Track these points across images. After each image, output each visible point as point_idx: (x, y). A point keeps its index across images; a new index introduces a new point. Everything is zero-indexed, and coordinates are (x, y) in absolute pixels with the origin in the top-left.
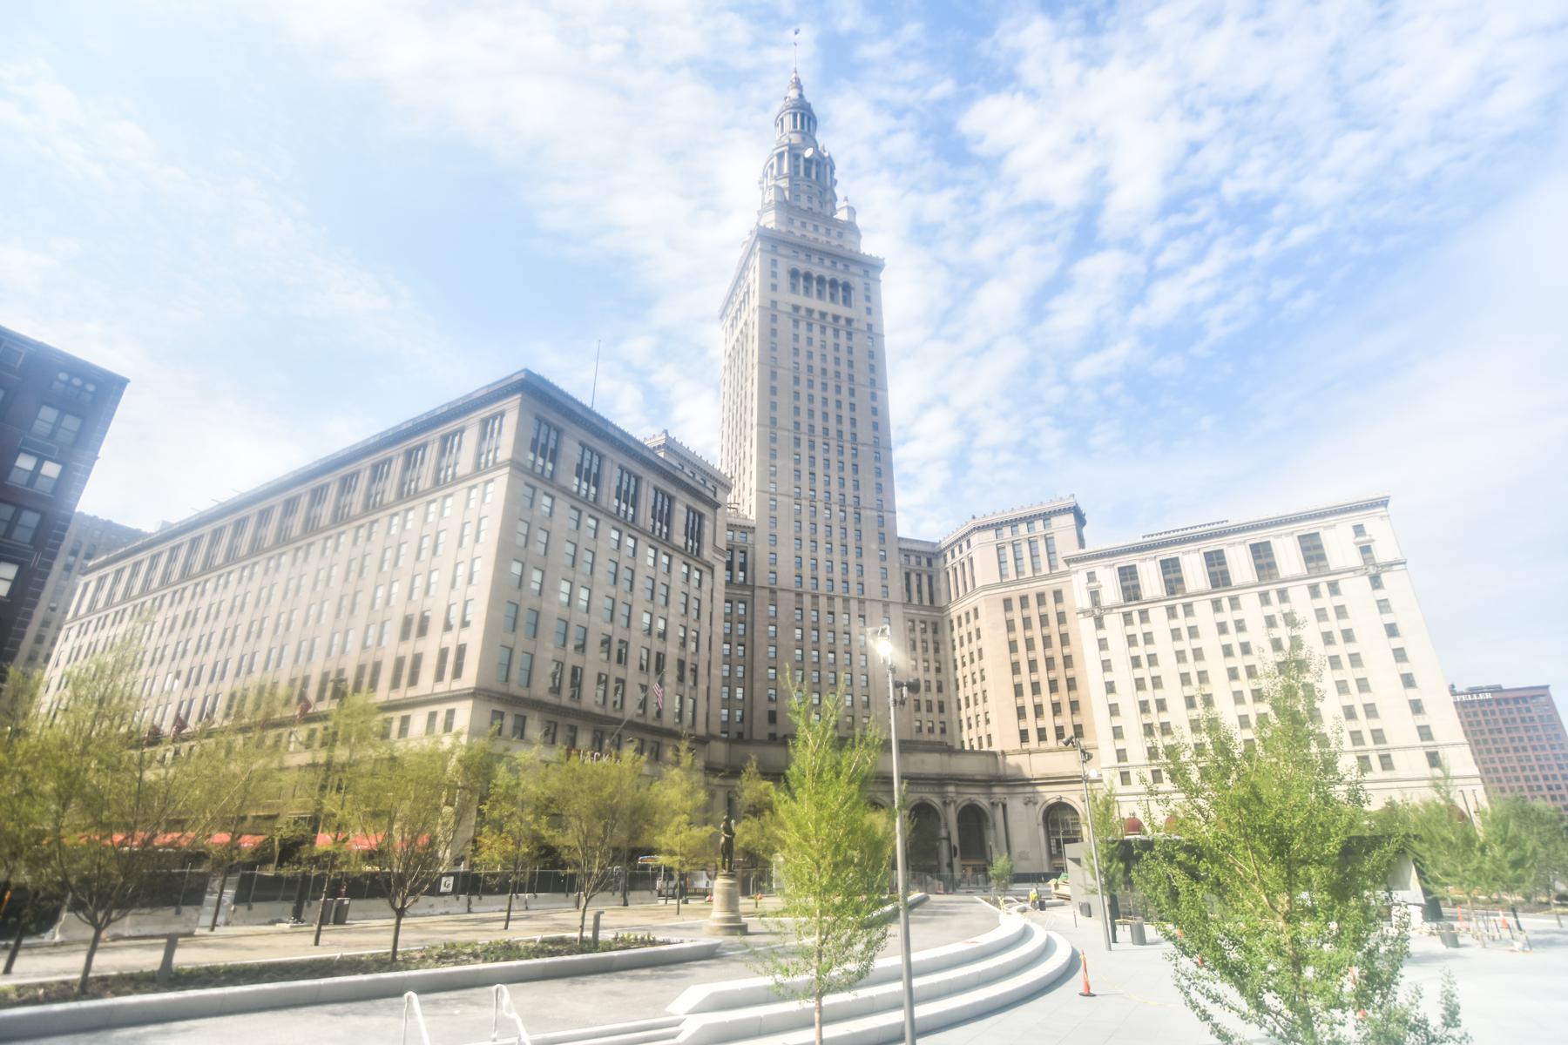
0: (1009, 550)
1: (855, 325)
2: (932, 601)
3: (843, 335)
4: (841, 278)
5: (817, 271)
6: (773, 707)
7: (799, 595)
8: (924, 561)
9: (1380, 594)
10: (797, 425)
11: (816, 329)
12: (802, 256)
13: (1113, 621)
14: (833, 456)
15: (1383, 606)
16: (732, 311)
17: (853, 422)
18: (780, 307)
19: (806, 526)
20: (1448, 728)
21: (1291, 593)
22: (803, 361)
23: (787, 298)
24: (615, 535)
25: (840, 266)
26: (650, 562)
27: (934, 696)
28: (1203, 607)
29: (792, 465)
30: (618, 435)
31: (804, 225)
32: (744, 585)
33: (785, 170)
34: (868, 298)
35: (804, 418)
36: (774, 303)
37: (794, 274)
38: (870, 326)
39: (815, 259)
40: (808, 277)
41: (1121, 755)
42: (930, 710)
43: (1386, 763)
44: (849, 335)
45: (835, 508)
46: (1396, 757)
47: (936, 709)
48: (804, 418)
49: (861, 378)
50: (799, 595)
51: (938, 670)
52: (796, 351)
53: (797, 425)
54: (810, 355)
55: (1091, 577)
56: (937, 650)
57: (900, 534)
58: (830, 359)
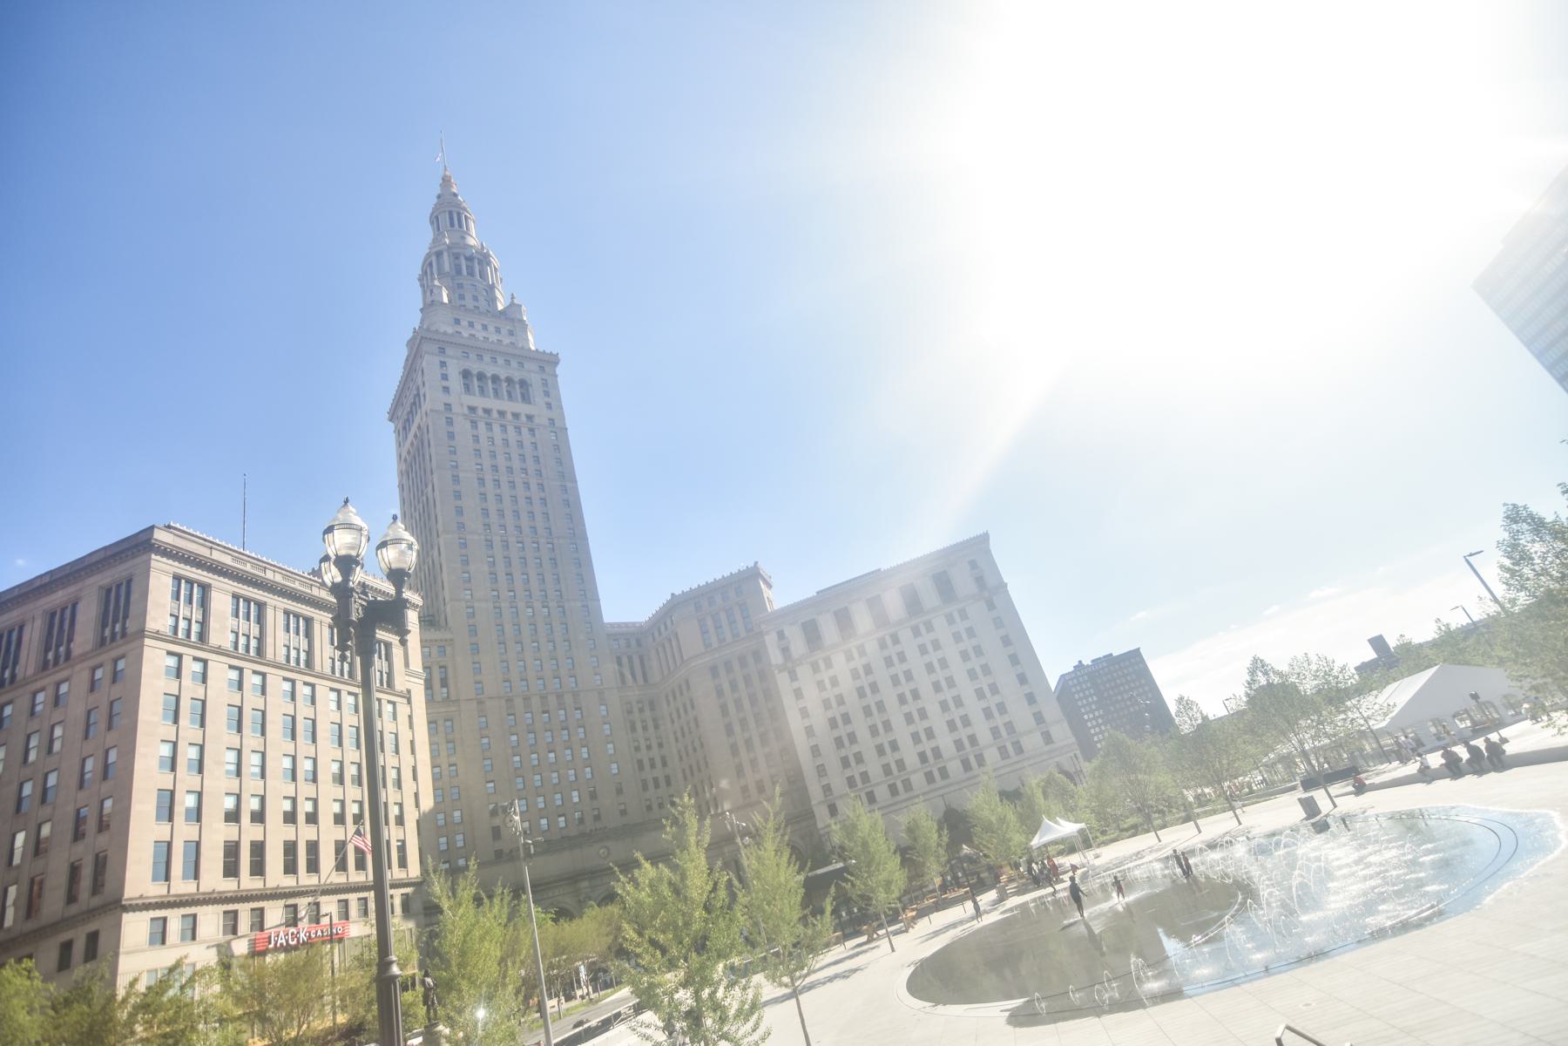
0: (709, 622)
1: (537, 420)
2: (645, 680)
3: (525, 431)
4: (517, 376)
5: (490, 371)
6: (497, 821)
7: (509, 700)
8: (633, 643)
10: (487, 526)
11: (496, 428)
12: (473, 356)
13: (804, 671)
15: (998, 623)
16: (402, 413)
18: (456, 409)
19: (508, 628)
20: (1052, 711)
22: (487, 462)
23: (461, 400)
24: (287, 686)
25: (514, 363)
26: (333, 706)
27: (659, 772)
29: (486, 568)
30: (278, 578)
31: (471, 325)
33: (447, 267)
34: (547, 394)
35: (494, 518)
36: (448, 406)
37: (466, 374)
38: (552, 421)
39: (487, 358)
40: (481, 376)
41: (827, 789)
42: (657, 786)
43: (1019, 750)
44: (532, 430)
45: (538, 605)
46: (1026, 742)
47: (662, 783)
48: (494, 518)
50: (509, 700)
51: (660, 745)
52: (478, 452)
53: (487, 526)
54: (493, 455)
55: (781, 635)
56: (656, 727)
58: (515, 456)
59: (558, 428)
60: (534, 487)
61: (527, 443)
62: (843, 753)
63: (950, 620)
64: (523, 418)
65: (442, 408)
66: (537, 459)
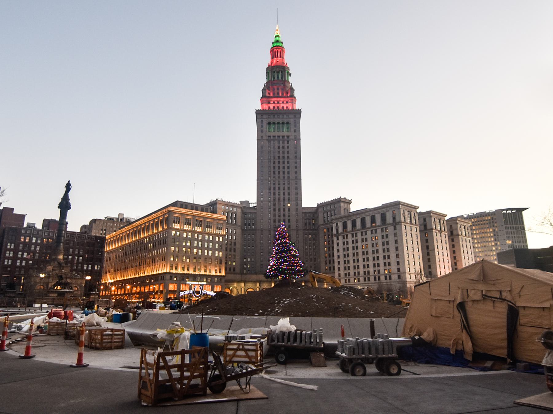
1: (290, 138)
3: (286, 142)
7: (270, 231)
8: (312, 216)
9: (395, 231)
12: (272, 116)
13: (340, 237)
14: (282, 186)
15: (395, 235)
17: (288, 173)
21: (378, 230)
28: (359, 234)
29: (268, 191)
32: (253, 230)
37: (269, 123)
39: (276, 116)
40: (274, 123)
41: (339, 275)
49: (292, 156)
57: (303, 206)
58: (281, 152)
59: (298, 139)
60: (286, 163)
61: (286, 147)
62: (345, 265)
63: (382, 230)
64: (286, 138)
65: (260, 138)
66: (288, 152)
